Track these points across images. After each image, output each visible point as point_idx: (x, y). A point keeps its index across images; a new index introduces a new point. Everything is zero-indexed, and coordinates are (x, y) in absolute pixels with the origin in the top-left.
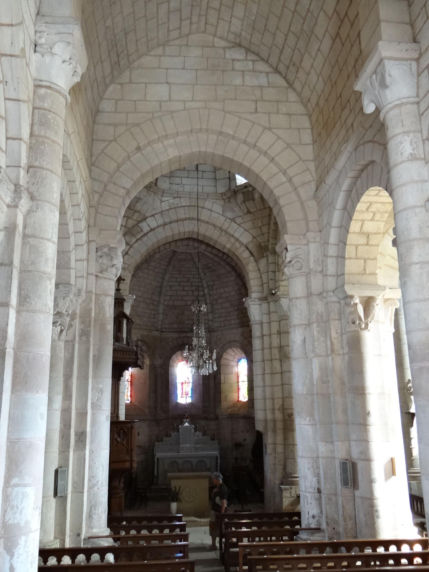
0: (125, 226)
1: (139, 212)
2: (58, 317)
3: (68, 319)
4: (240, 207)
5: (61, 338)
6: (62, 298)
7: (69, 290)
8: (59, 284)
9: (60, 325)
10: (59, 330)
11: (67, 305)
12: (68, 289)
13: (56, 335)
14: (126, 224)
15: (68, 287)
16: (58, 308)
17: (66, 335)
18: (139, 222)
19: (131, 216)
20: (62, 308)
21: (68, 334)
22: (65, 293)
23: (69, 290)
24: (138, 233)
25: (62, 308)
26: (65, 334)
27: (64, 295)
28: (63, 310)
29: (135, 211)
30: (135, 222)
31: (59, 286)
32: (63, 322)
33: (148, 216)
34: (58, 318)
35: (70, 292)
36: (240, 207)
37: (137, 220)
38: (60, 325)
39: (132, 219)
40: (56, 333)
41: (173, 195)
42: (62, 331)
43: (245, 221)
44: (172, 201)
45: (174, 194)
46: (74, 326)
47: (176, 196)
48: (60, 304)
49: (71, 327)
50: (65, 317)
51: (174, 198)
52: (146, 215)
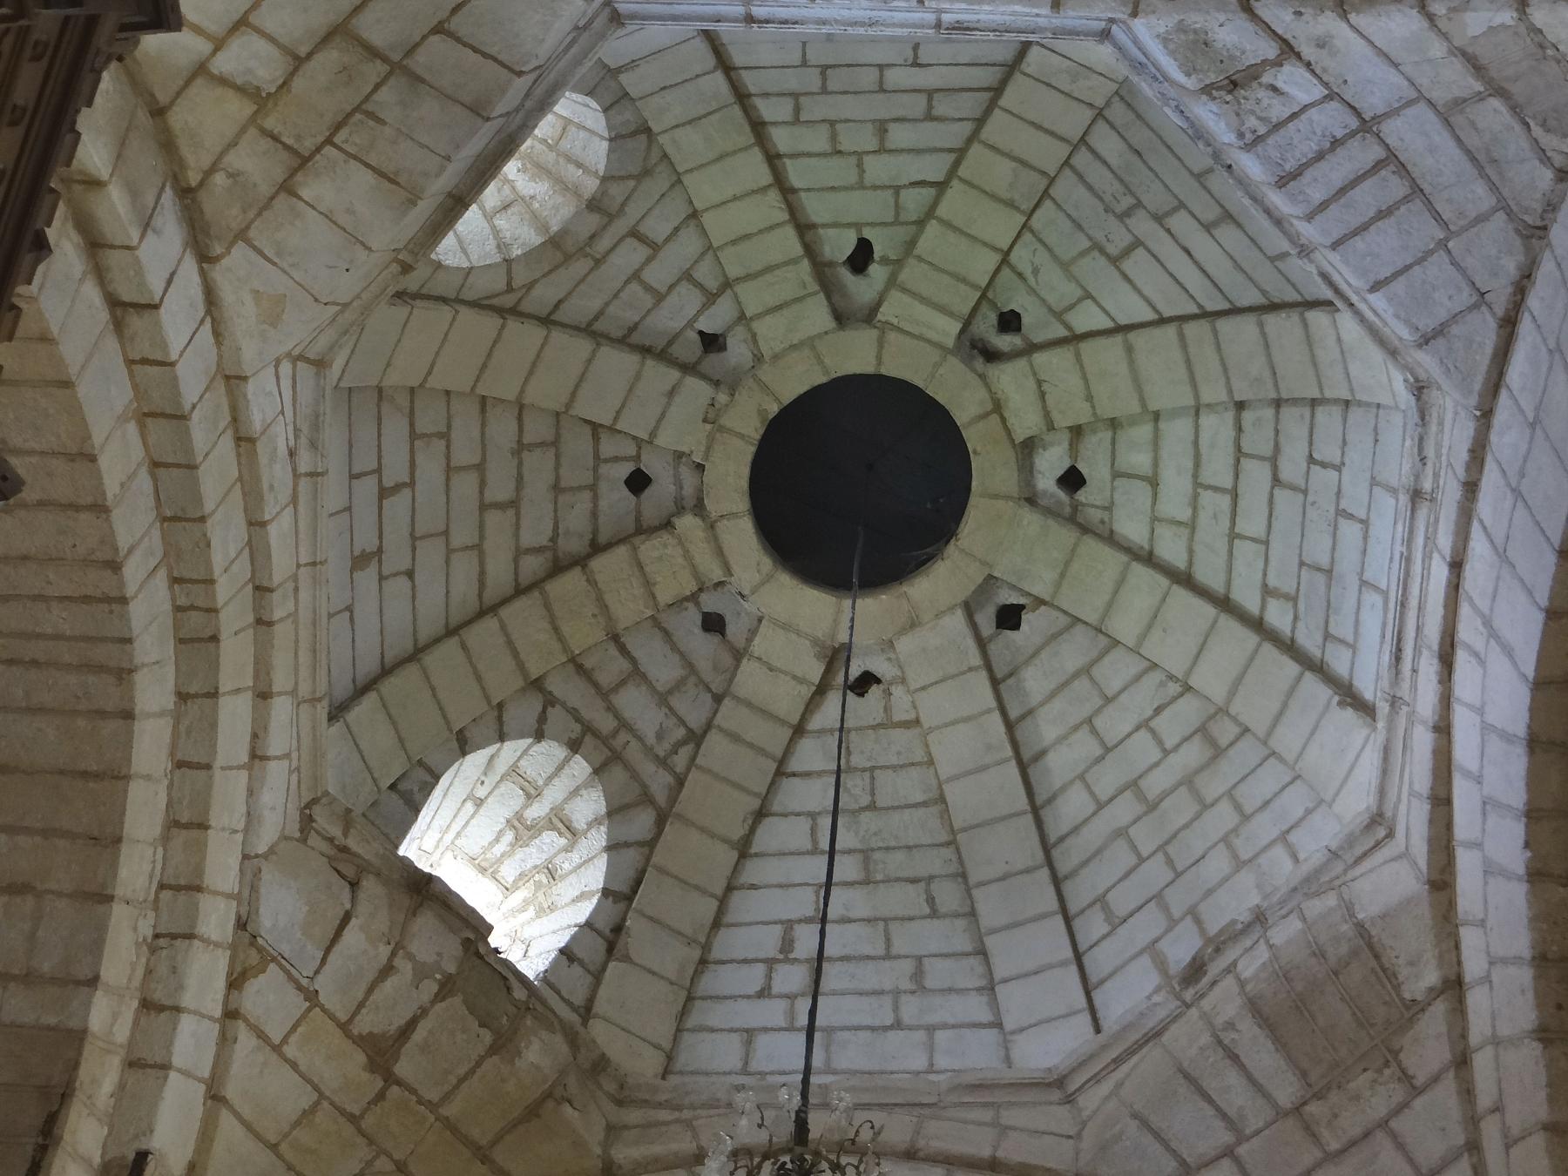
0: (201, 69)
1: (287, 187)
4: (387, 970)
14: (223, 81)
18: (186, 194)
19: (270, 123)
24: (134, 193)
29: (303, 161)
30: (195, 162)
33: (218, 273)
36: (387, 970)
37: (219, 179)
39: (243, 130)
41: (303, 440)
43: (290, 1051)
44: (282, 450)
45: (313, 445)
47: (303, 469)
51: (292, 453)
52: (240, 250)
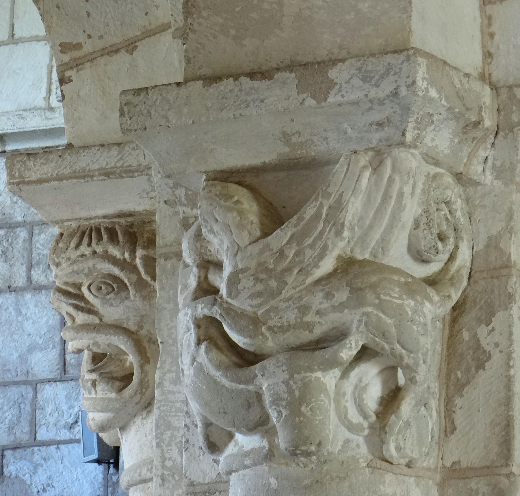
2: (342, 295)
3: (433, 310)
5: (391, 450)
6: (364, 160)
7: (395, 94)
8: (334, 62)
9: (364, 354)
10: (374, 392)
11: (412, 209)
12: (387, 87)
13: (351, 427)
15: (387, 72)
16: (339, 233)
17: (449, 428)
20: (377, 235)
21: (459, 418)
22: (377, 116)
23: (395, 94)
25: (377, 235)
26: (433, 422)
27: (376, 137)
28: (384, 243)
31: (333, 73)
32: (384, 335)
34: (341, 307)
35: (406, 110)
38: (364, 354)
40: (354, 416)
42: (392, 397)
46: (497, 359)
48: (354, 207)
49: (480, 366)
50: (394, 296)
